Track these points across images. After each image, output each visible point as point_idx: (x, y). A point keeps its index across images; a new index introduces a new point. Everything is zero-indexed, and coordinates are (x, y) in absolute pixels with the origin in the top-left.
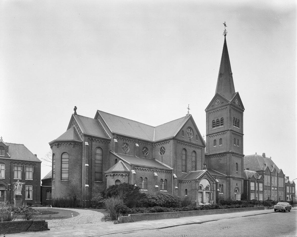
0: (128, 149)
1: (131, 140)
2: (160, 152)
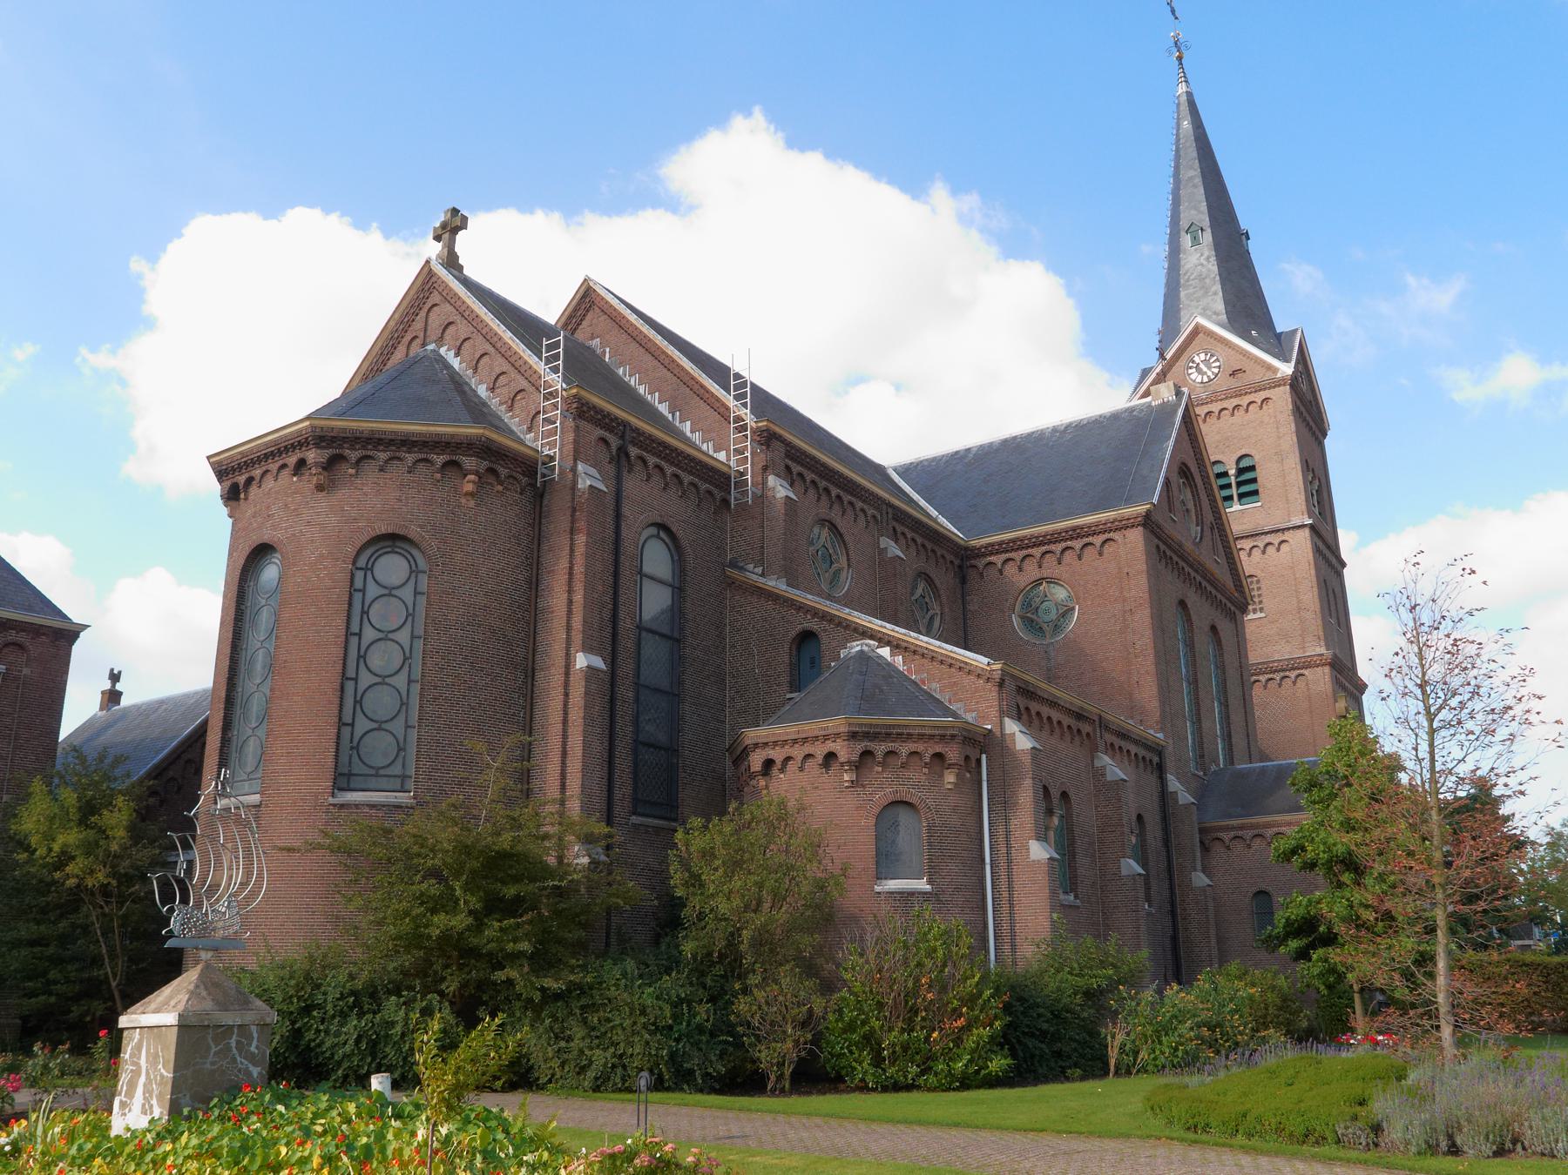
0: (839, 571)
2: (1022, 617)
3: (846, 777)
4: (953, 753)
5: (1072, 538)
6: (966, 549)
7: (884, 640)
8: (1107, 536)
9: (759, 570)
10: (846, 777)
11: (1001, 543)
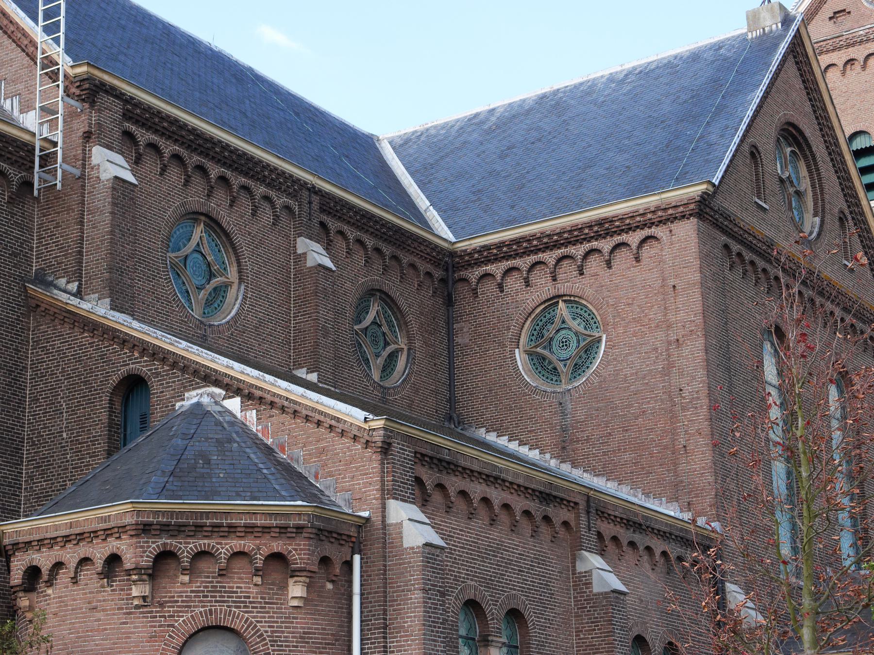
0: (227, 286)
1: (260, 190)
2: (530, 354)
3: (135, 591)
4: (300, 552)
5: (598, 237)
6: (452, 254)
7: (233, 388)
8: (646, 232)
9: (73, 287)
10: (135, 591)
11: (500, 245)
